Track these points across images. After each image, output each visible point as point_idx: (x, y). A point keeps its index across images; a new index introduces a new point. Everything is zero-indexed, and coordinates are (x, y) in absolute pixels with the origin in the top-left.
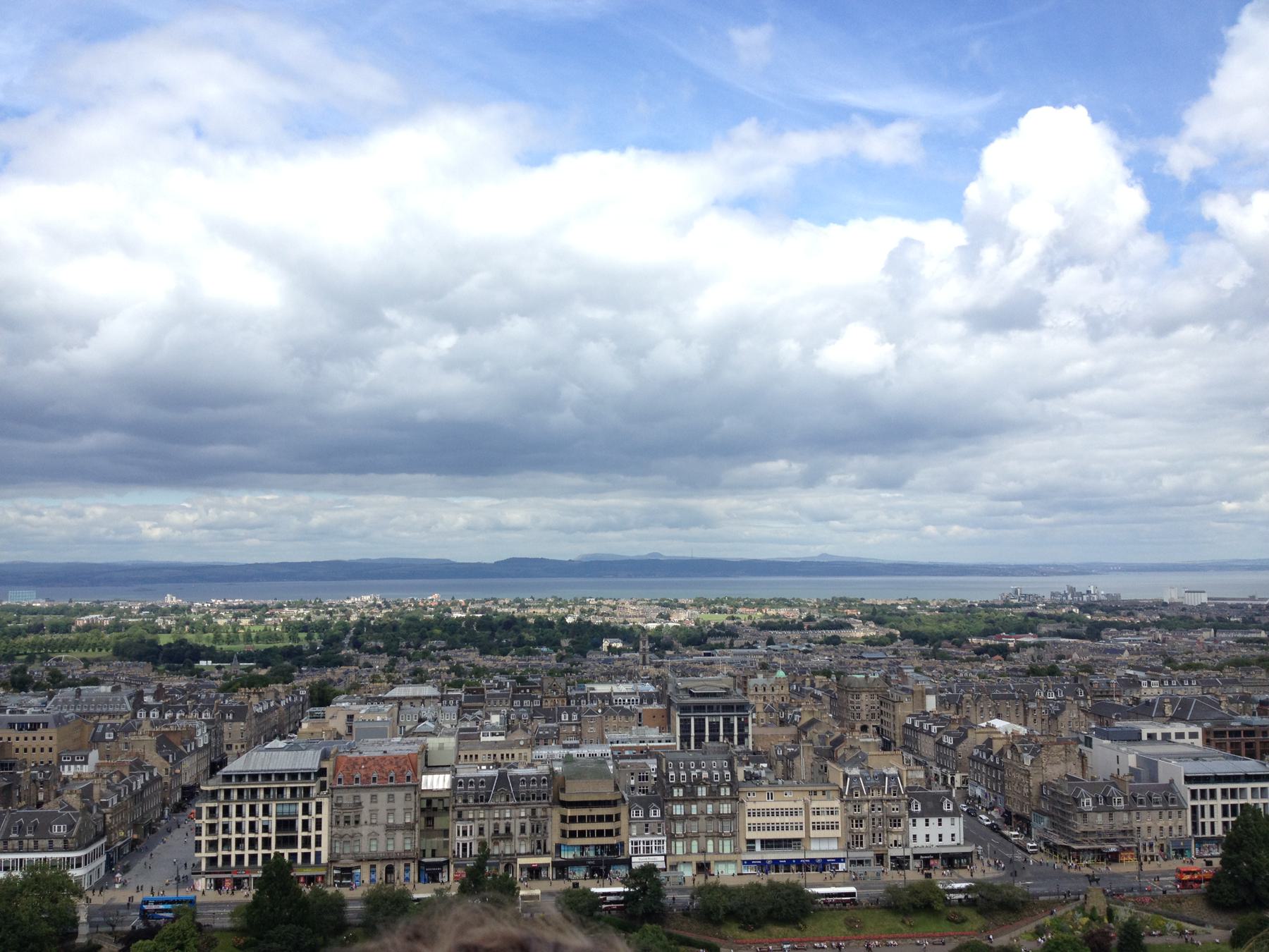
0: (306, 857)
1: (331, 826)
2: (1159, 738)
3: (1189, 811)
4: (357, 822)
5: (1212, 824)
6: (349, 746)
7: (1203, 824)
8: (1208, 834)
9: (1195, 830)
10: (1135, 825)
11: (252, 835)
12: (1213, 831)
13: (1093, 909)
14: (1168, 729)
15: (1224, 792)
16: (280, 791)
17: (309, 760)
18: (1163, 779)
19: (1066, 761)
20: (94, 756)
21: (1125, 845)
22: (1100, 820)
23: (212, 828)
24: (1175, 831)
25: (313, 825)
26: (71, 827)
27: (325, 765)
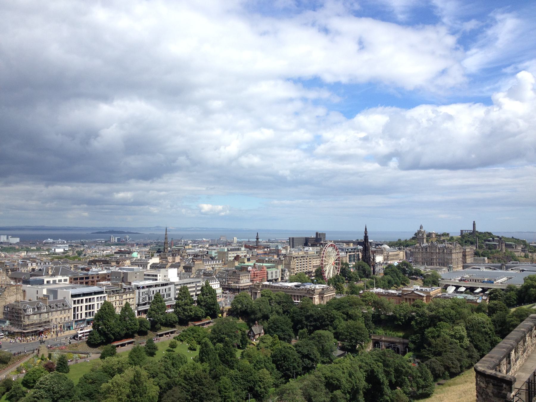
2: (51, 282)
3: (73, 310)
5: (81, 314)
7: (78, 314)
8: (79, 318)
9: (74, 318)
10: (50, 318)
12: (81, 317)
13: (43, 355)
14: (54, 279)
15: (86, 299)
18: (60, 298)
19: (17, 294)
21: (47, 327)
22: (35, 318)
24: (67, 319)
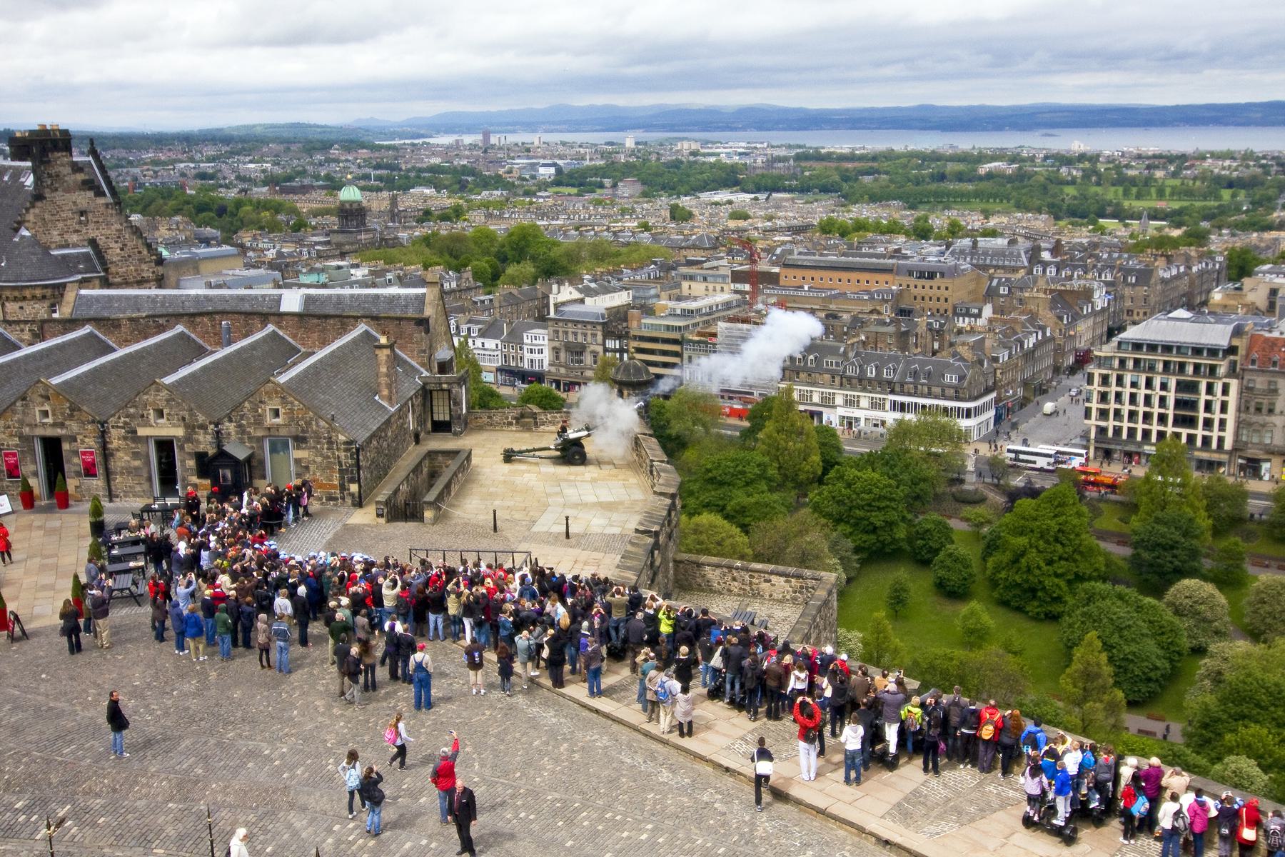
0: (1206, 441)
1: (1239, 410)
4: (1271, 411)
6: (1269, 324)
11: (1147, 409)
16: (1182, 366)
17: (1218, 335)
20: (988, 311)
23: (1104, 397)
25: (1217, 407)
26: (962, 378)
27: (1236, 342)
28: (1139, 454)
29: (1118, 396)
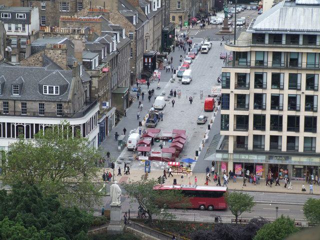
11: (293, 113)
26: (64, 89)
28: (285, 167)
29: (259, 98)
